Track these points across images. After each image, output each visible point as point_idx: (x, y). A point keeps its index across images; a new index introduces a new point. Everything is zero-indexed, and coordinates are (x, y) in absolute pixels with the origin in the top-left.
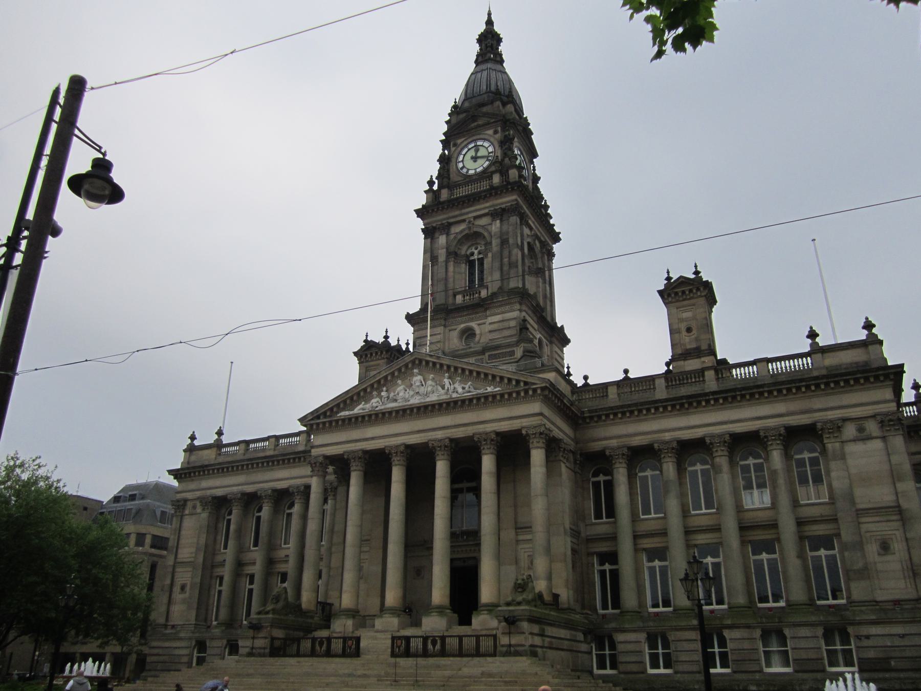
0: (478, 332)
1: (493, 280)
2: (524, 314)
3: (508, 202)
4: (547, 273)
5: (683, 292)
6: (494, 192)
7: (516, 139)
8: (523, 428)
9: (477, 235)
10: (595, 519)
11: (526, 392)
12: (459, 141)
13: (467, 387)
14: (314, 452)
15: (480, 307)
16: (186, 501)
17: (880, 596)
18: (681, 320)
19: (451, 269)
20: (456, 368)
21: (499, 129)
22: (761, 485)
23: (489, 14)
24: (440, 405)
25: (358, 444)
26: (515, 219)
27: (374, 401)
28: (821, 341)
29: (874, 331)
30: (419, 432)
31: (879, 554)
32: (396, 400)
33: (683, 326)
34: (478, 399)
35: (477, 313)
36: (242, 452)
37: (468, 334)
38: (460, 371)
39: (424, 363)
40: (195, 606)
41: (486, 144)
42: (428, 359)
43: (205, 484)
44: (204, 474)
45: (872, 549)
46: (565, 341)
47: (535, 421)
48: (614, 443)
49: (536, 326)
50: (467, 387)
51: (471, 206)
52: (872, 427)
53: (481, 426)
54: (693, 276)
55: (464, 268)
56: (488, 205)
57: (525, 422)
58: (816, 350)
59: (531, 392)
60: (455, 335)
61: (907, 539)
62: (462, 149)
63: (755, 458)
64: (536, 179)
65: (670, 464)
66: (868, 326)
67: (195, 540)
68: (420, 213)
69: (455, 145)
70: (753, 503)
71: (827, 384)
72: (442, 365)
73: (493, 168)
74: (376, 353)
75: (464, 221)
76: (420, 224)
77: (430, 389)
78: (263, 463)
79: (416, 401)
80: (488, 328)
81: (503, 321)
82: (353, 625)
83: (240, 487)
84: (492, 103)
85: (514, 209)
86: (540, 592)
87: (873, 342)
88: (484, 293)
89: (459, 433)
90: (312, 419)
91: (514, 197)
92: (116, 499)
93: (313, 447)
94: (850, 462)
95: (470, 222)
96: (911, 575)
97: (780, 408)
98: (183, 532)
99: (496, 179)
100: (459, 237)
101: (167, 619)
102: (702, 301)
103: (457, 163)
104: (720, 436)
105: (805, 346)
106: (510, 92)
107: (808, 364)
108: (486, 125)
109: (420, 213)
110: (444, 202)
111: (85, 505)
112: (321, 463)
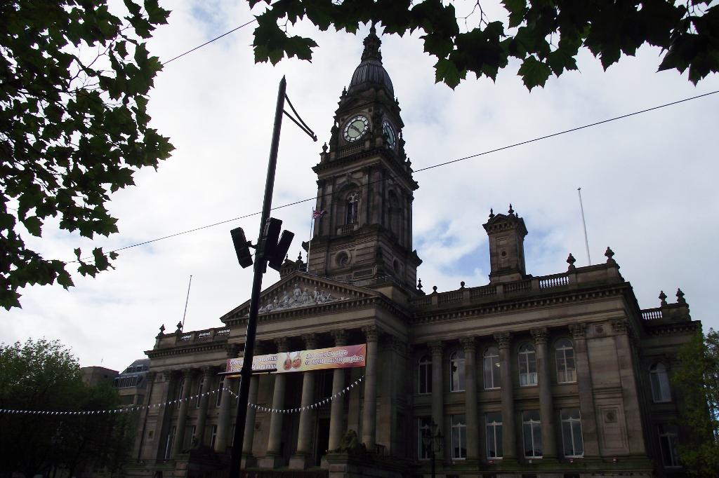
0: (349, 256)
1: (362, 218)
2: (380, 243)
3: (374, 162)
4: (406, 210)
5: (500, 226)
6: (366, 154)
7: (385, 115)
8: (363, 327)
9: (354, 186)
10: (421, 392)
12: (346, 117)
13: (328, 297)
14: (231, 341)
15: (350, 238)
16: (155, 373)
17: (606, 453)
18: (498, 247)
19: (335, 210)
20: (322, 284)
21: (372, 108)
22: (532, 370)
24: (310, 309)
26: (377, 174)
27: (269, 306)
28: (577, 265)
29: (613, 257)
31: (606, 422)
32: (282, 306)
33: (500, 251)
34: (335, 306)
36: (193, 338)
37: (343, 257)
38: (324, 286)
39: (302, 279)
40: (157, 448)
41: (363, 119)
43: (169, 361)
44: (167, 355)
45: (602, 418)
46: (419, 262)
47: (372, 322)
48: (433, 337)
49: (390, 252)
50: (328, 297)
52: (607, 328)
53: (336, 325)
54: (508, 214)
55: (344, 209)
56: (361, 163)
57: (365, 323)
58: (572, 270)
59: (368, 302)
60: (334, 257)
61: (625, 412)
63: (566, 346)
64: (402, 143)
65: (470, 354)
66: (609, 253)
68: (316, 169)
70: (527, 384)
71: (577, 297)
72: (313, 281)
73: (366, 137)
75: (344, 175)
76: (315, 177)
77: (304, 298)
78: (204, 348)
79: (294, 306)
80: (355, 253)
82: (246, 463)
83: (190, 365)
84: (369, 89)
85: (379, 167)
86: (364, 444)
87: (612, 264)
88: (356, 228)
91: (378, 158)
92: (129, 370)
93: (229, 338)
94: (592, 354)
96: (626, 437)
97: (545, 313)
98: (153, 395)
99: (367, 144)
100: (341, 187)
101: (139, 457)
102: (513, 232)
103: (344, 133)
104: (503, 334)
105: (565, 268)
106: (383, 81)
107: (566, 281)
108: (363, 107)
109: (316, 169)
110: (333, 162)
111: (102, 374)
112: (234, 349)
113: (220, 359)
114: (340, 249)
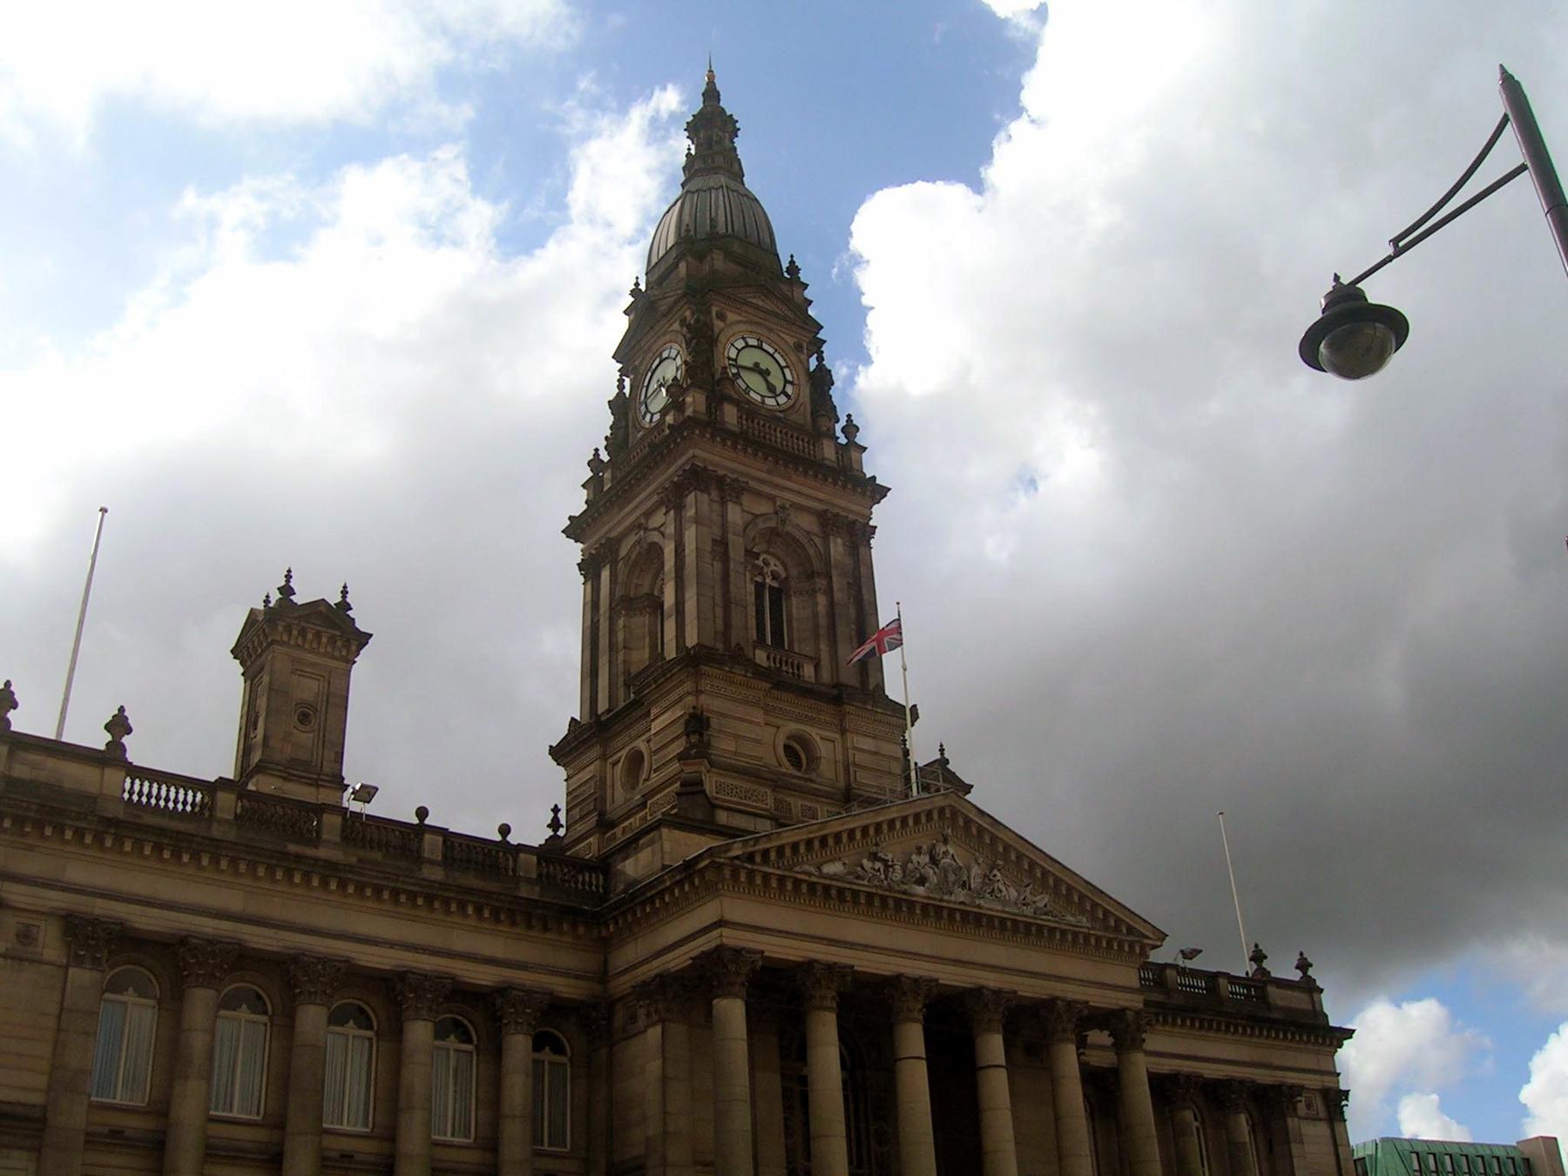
12: (731, 317)
25: (834, 949)
69: (721, 317)
75: (772, 499)
81: (876, 753)
83: (226, 926)
90: (737, 858)
95: (783, 507)
100: (761, 525)
113: (392, 945)
114: (797, 720)
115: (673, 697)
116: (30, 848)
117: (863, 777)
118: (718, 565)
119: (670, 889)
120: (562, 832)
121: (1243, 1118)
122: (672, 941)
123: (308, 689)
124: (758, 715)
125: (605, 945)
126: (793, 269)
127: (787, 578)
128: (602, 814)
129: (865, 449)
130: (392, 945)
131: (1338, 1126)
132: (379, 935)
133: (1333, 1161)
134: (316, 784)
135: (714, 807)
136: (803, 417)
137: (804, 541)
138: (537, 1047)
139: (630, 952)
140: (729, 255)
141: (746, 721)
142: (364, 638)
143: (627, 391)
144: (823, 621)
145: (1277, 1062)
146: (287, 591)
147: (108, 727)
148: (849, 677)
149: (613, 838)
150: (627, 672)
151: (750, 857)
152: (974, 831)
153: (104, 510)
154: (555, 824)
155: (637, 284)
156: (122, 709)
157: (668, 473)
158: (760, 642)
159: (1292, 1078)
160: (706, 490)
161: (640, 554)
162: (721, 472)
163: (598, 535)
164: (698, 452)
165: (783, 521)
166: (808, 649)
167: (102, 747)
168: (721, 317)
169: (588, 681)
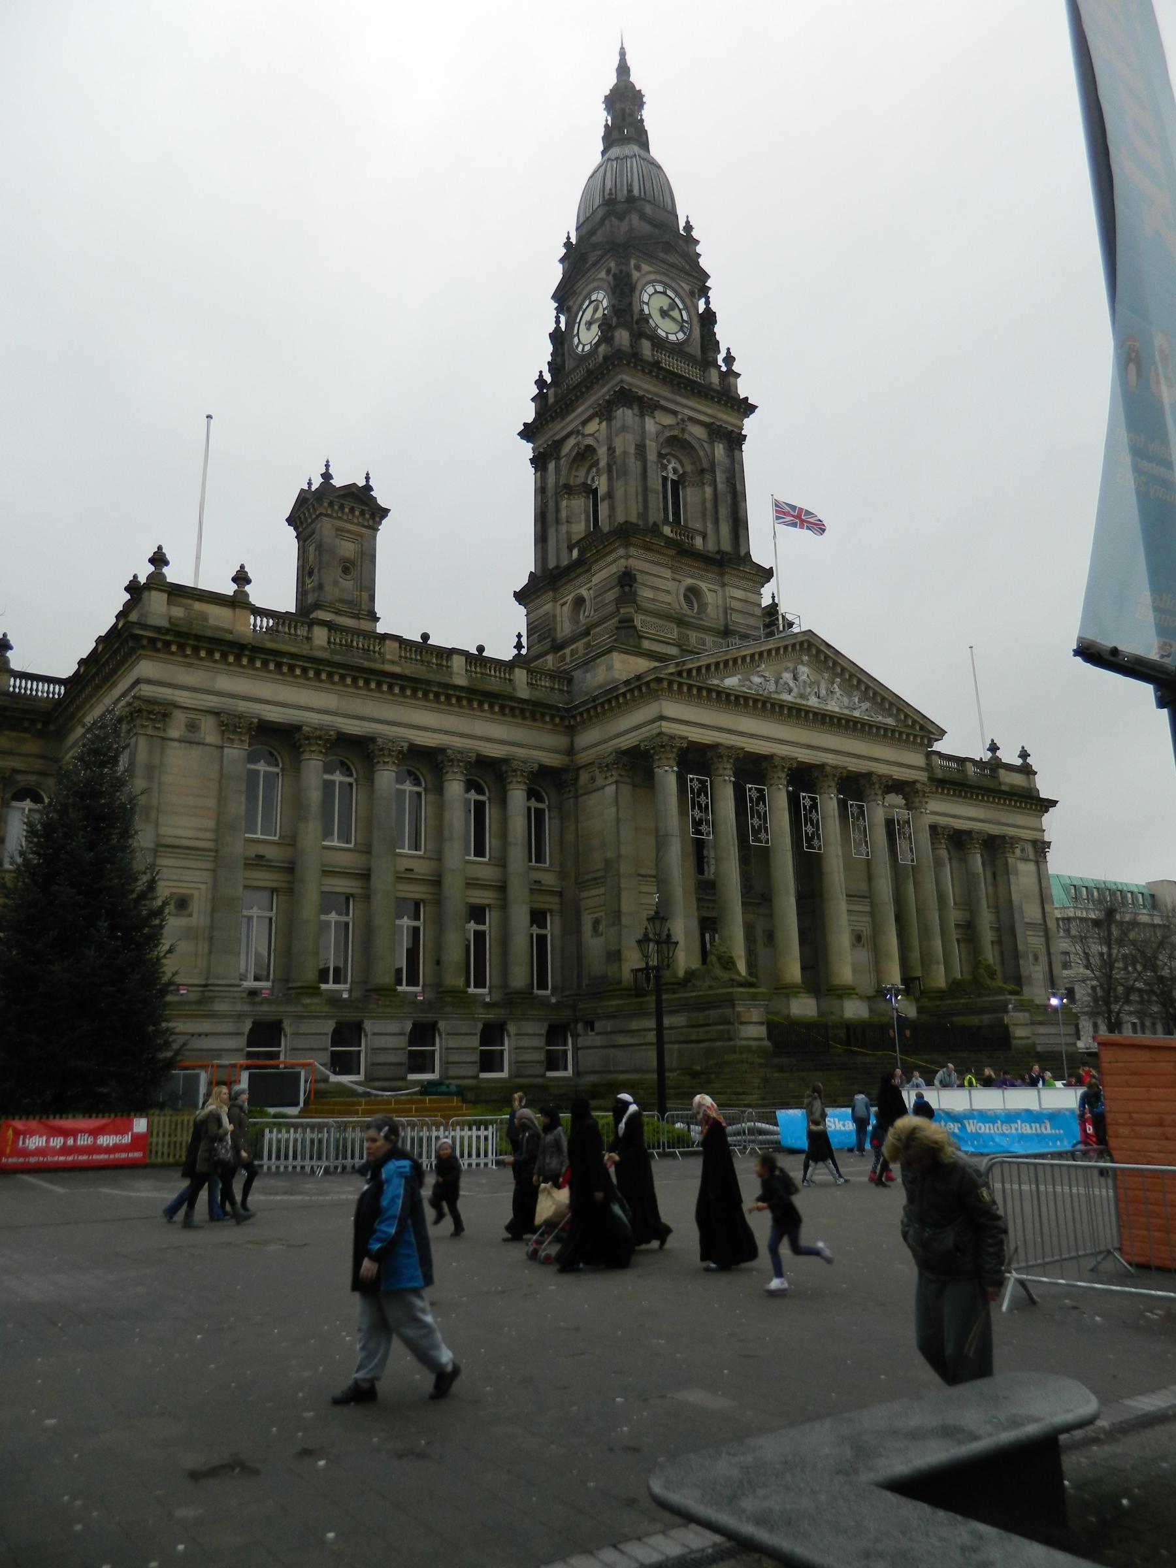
11: (922, 737)
12: (646, 268)
16: (176, 706)
23: (623, 54)
30: (809, 747)
35: (707, 571)
37: (693, 594)
42: (822, 648)
51: (687, 398)
56: (709, 411)
62: (647, 284)
66: (1024, 755)
67: (211, 803)
74: (362, 513)
75: (674, 413)
81: (745, 601)
87: (1027, 770)
89: (854, 765)
90: (672, 674)
100: (668, 434)
113: (434, 730)
115: (610, 559)
116: (190, 665)
117: (736, 617)
118: (639, 463)
119: (624, 694)
120: (524, 651)
121: (979, 856)
122: (628, 727)
123: (347, 549)
124: (668, 573)
125: (571, 731)
126: (689, 227)
127: (684, 473)
128: (553, 640)
129: (738, 375)
130: (434, 730)
131: (1042, 865)
132: (427, 724)
133: (1036, 888)
134: (357, 617)
135: (641, 637)
136: (695, 349)
137: (697, 446)
138: (529, 799)
139: (589, 737)
140: (643, 217)
141: (661, 577)
142: (384, 512)
143: (563, 326)
144: (709, 505)
145: (1004, 820)
146: (327, 476)
147: (234, 580)
148: (726, 546)
149: (563, 658)
150: (569, 539)
151: (680, 674)
152: (822, 658)
153: (209, 417)
154: (519, 646)
155: (568, 238)
156: (242, 567)
157: (602, 393)
158: (666, 521)
159: (1012, 832)
160: (630, 407)
161: (578, 453)
162: (641, 393)
163: (544, 440)
164: (625, 377)
165: (683, 430)
166: (698, 526)
167: (231, 594)
168: (638, 268)
169: (540, 546)
